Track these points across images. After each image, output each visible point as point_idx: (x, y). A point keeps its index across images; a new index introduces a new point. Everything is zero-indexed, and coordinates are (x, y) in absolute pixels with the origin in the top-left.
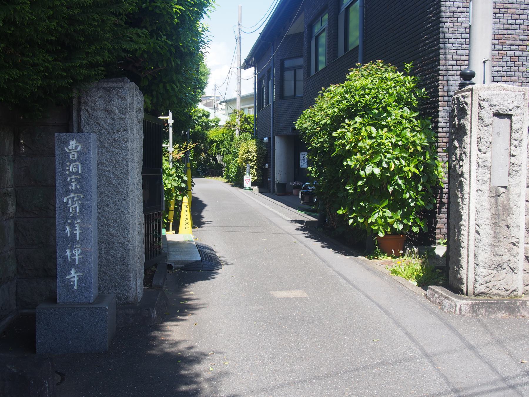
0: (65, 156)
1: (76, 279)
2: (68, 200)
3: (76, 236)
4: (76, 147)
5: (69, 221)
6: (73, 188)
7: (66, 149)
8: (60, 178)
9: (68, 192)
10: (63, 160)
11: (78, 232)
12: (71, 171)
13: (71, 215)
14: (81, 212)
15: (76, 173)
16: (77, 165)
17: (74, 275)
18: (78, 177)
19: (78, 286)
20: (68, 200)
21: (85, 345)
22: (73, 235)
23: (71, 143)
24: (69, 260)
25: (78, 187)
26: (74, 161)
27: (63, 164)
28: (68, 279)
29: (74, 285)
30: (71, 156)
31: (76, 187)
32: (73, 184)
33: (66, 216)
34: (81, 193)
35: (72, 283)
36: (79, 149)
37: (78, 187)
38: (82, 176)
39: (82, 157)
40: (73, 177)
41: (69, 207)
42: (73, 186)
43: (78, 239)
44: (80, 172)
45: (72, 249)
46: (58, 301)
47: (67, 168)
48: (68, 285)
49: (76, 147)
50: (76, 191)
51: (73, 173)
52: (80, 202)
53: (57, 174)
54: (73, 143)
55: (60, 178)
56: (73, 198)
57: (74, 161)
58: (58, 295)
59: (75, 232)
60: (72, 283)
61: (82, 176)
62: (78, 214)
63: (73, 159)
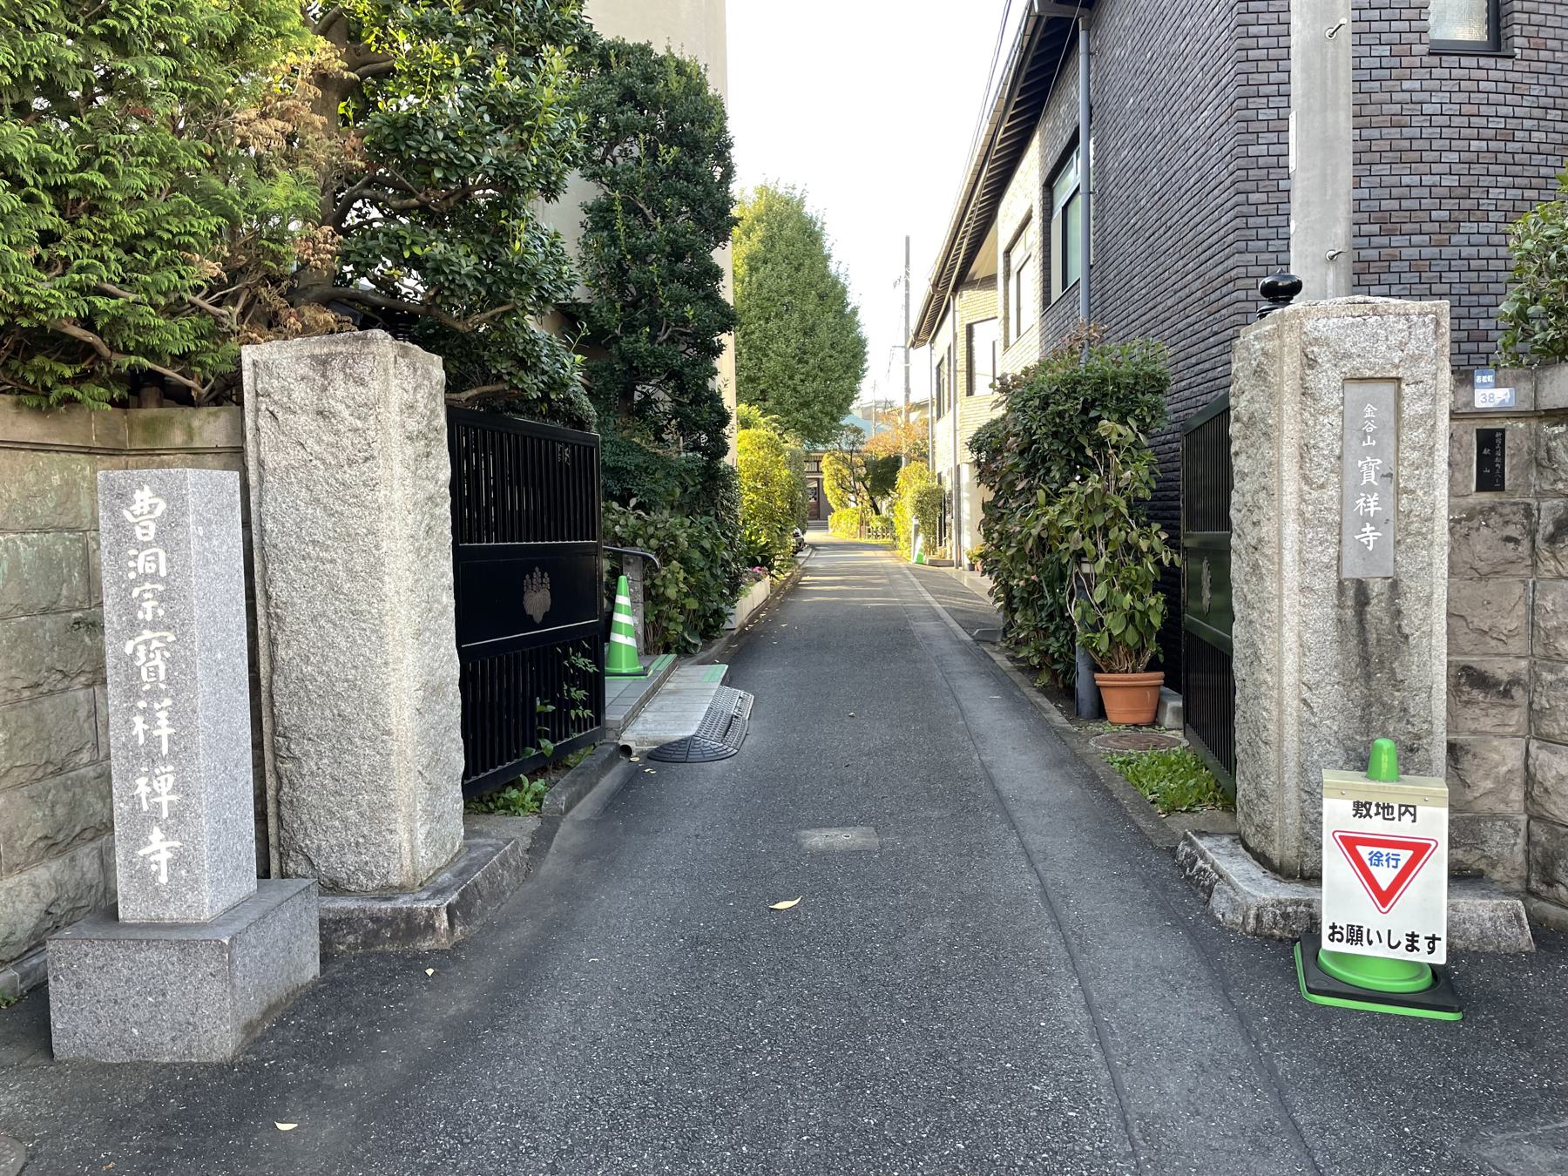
0: (124, 533)
1: (164, 857)
2: (135, 650)
3: (160, 742)
4: (153, 507)
5: (142, 704)
6: (149, 617)
7: (126, 513)
8: (113, 590)
9: (134, 627)
10: (118, 543)
11: (164, 731)
12: (141, 571)
13: (147, 687)
14: (168, 681)
15: (154, 578)
16: (156, 555)
17: (158, 848)
18: (160, 588)
19: (171, 877)
20: (135, 650)
21: (173, 1039)
22: (154, 742)
23: (138, 495)
24: (145, 807)
25: (161, 612)
26: (147, 545)
27: (118, 554)
28: (144, 857)
29: (158, 873)
30: (138, 531)
31: (155, 615)
32: (148, 605)
33: (132, 692)
34: (168, 628)
35: (154, 868)
36: (158, 513)
37: (161, 612)
38: (168, 583)
39: (169, 529)
40: (148, 586)
41: (139, 669)
42: (148, 611)
43: (165, 751)
44: (163, 573)
45: (151, 776)
46: (121, 916)
47: (131, 564)
48: (144, 875)
49: (153, 507)
50: (154, 626)
51: (146, 577)
52: (167, 655)
53: (104, 581)
54: (143, 498)
55: (113, 590)
56: (147, 643)
57: (147, 545)
58: (120, 898)
59: (156, 733)
60: (154, 868)
61: (168, 583)
62: (163, 686)
63: (146, 539)
